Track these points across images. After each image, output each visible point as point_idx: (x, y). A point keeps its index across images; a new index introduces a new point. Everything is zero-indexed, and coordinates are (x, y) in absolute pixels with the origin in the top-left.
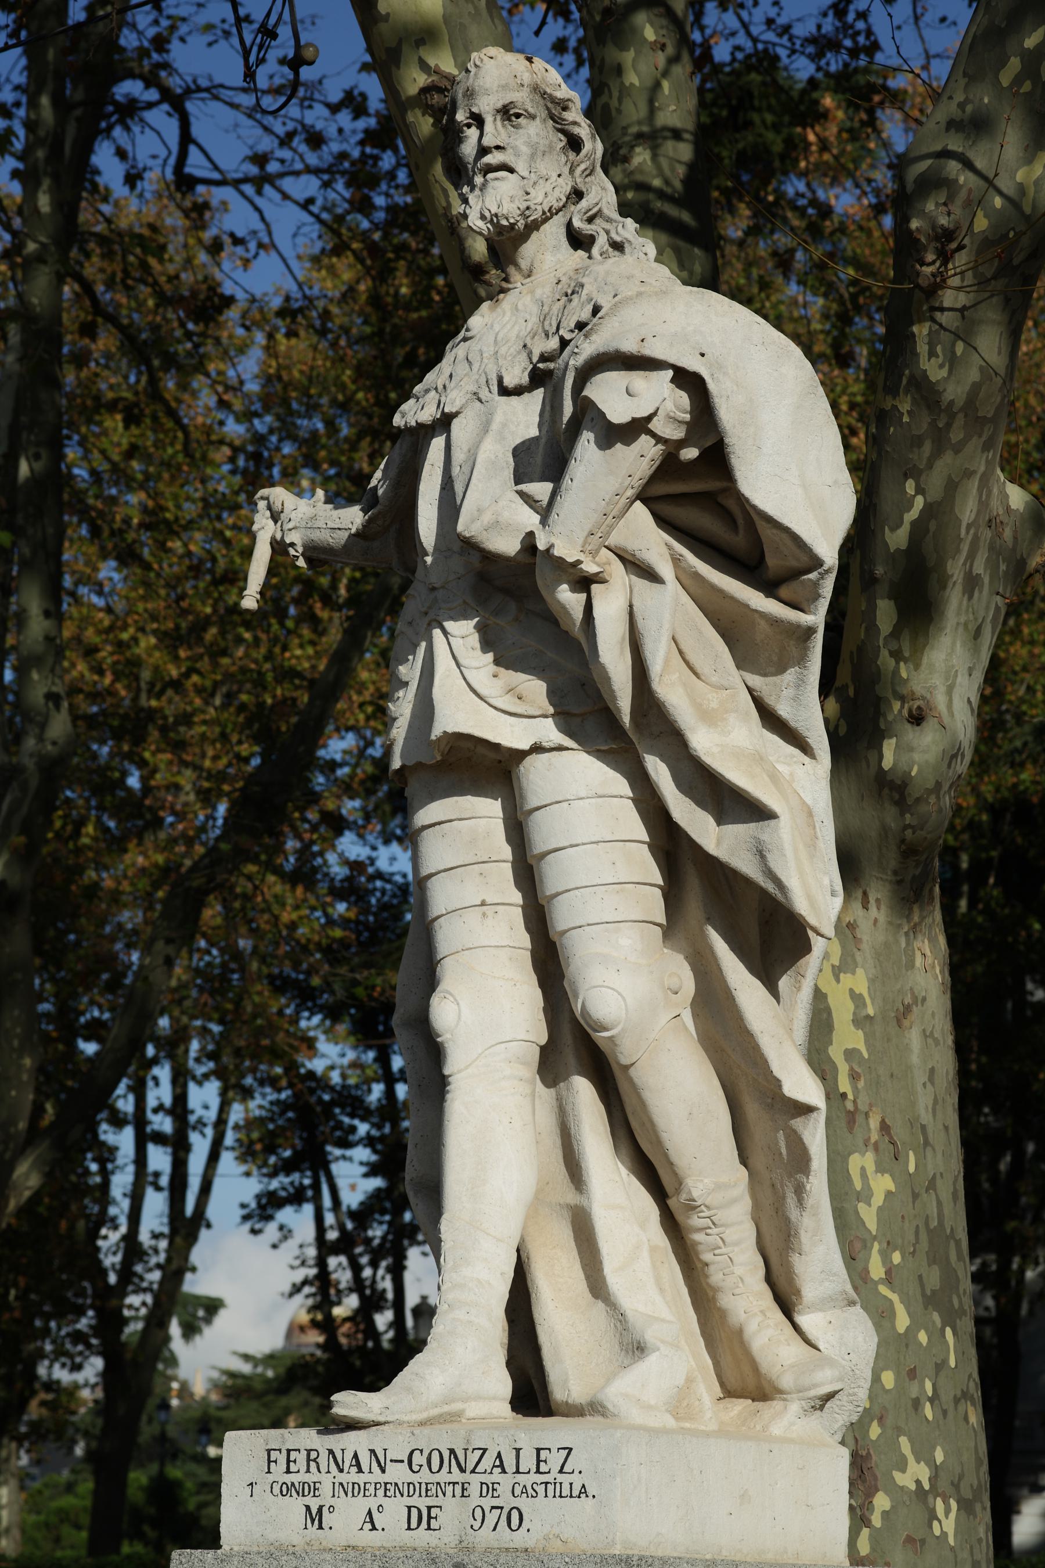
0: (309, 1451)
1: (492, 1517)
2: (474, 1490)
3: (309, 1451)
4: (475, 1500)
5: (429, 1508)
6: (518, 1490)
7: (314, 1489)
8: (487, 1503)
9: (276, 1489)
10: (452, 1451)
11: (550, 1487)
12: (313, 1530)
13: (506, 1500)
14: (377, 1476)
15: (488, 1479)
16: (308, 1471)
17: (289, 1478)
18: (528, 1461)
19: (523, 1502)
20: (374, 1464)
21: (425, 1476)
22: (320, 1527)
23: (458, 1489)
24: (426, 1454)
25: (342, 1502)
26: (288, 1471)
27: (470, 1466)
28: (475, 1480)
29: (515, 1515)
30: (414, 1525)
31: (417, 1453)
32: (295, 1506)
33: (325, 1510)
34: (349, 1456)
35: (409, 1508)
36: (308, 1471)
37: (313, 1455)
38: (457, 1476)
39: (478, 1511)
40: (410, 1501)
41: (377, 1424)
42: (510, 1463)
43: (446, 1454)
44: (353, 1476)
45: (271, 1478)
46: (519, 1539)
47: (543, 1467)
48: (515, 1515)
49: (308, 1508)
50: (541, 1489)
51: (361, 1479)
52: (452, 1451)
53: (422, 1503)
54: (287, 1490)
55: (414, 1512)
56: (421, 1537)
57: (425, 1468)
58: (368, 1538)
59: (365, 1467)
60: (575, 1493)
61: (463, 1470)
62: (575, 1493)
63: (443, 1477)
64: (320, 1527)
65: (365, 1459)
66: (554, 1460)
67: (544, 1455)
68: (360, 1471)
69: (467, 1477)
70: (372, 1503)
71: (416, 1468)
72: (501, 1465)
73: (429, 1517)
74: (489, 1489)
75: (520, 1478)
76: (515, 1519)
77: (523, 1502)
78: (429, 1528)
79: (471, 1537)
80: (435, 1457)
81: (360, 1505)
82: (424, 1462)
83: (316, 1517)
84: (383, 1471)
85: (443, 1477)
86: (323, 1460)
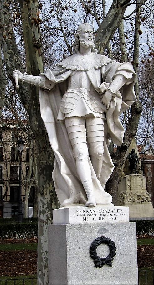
1: (112, 218)
2: (109, 215)
7: (84, 215)
8: (111, 216)
9: (78, 215)
13: (113, 216)
14: (94, 213)
17: (80, 214)
18: (116, 211)
19: (116, 216)
23: (107, 215)
25: (88, 217)
27: (108, 212)
28: (109, 213)
29: (115, 218)
32: (81, 218)
33: (86, 218)
34: (90, 211)
37: (84, 211)
38: (106, 213)
40: (99, 217)
41: (94, 206)
42: (114, 211)
43: (104, 211)
45: (77, 214)
46: (115, 221)
48: (115, 218)
51: (92, 214)
54: (80, 215)
60: (123, 215)
63: (104, 213)
66: (120, 211)
67: (118, 210)
69: (108, 213)
70: (93, 217)
77: (116, 216)
80: (103, 211)
81: (92, 217)
83: (85, 219)
85: (104, 213)
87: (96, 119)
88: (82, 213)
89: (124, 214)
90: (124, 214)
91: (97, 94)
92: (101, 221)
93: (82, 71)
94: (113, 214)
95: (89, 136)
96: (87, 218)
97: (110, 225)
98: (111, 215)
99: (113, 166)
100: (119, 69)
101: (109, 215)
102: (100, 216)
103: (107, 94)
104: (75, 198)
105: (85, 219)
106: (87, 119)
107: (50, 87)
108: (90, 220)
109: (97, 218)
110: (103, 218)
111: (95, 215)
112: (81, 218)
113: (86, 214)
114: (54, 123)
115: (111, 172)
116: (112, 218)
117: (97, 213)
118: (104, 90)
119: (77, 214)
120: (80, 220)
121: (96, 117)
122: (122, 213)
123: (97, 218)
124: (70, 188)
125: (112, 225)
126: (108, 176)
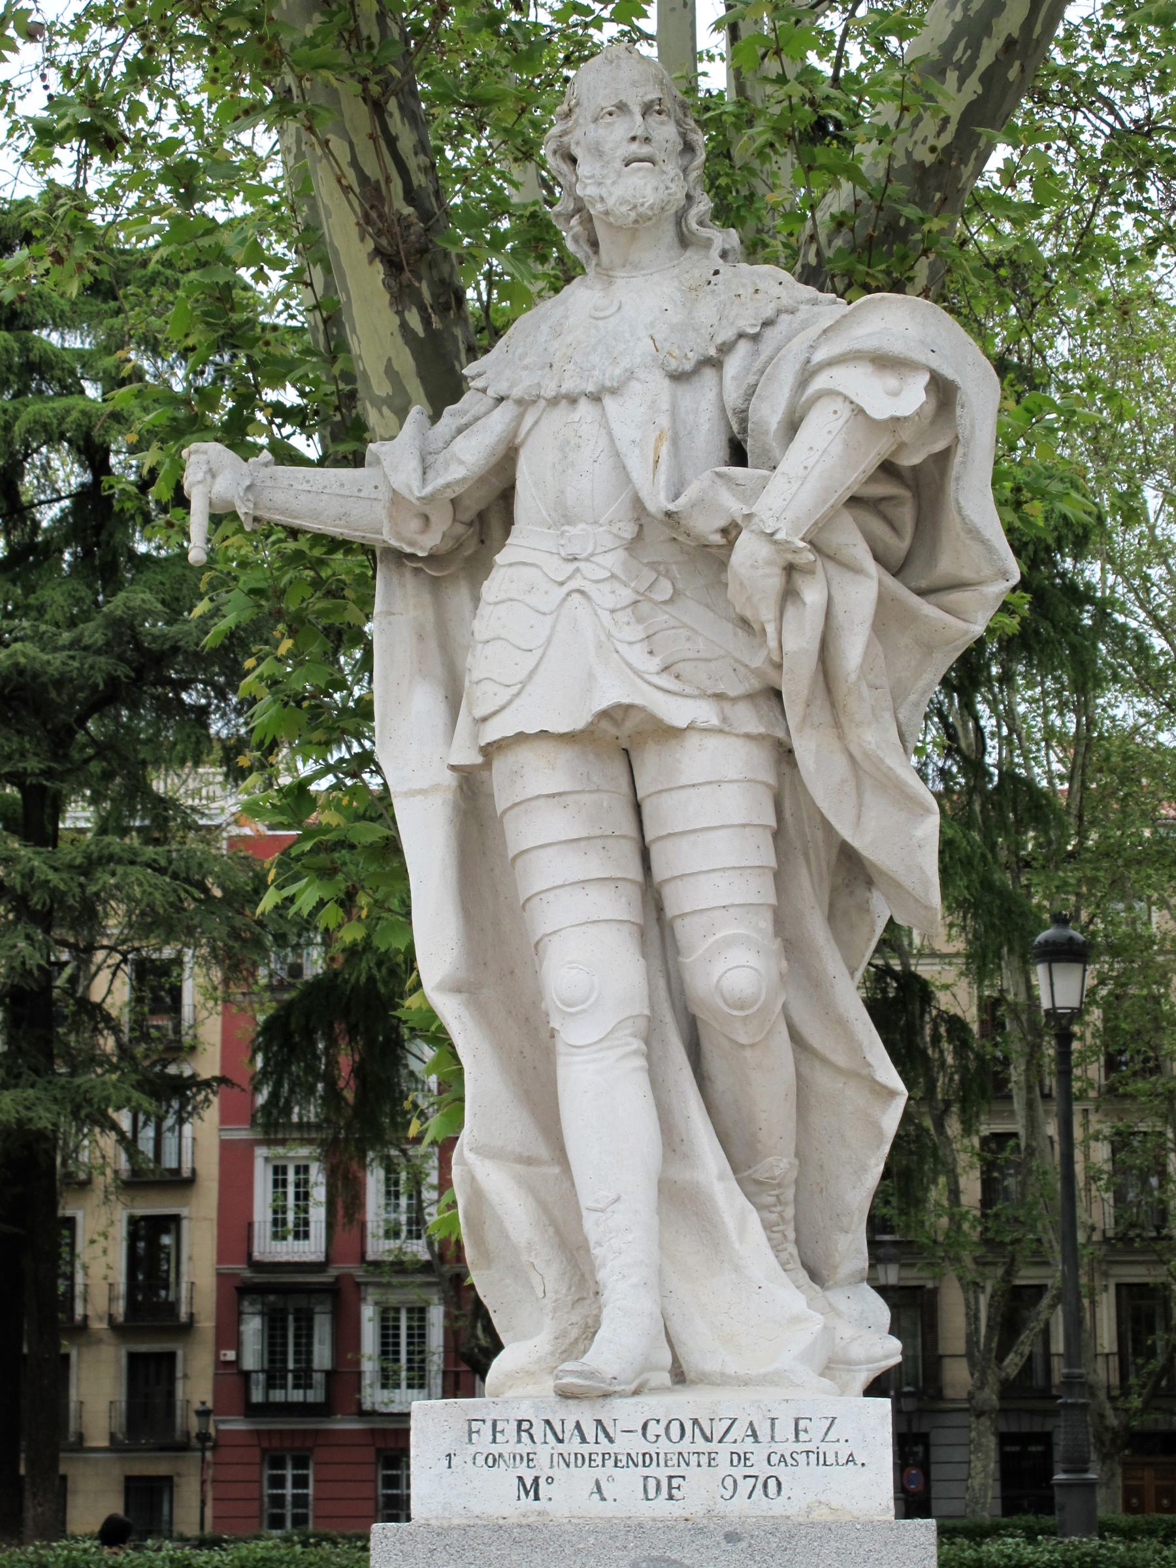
0: (520, 1422)
1: (745, 1486)
2: (723, 1459)
3: (520, 1422)
4: (724, 1467)
5: (670, 1478)
6: (775, 1459)
8: (739, 1472)
9: (480, 1460)
10: (695, 1422)
11: (813, 1457)
12: (528, 1502)
13: (761, 1469)
15: (739, 1448)
16: (519, 1441)
17: (495, 1449)
18: (785, 1430)
19: (781, 1471)
20: (601, 1435)
21: (664, 1446)
22: (537, 1498)
23: (704, 1460)
24: (663, 1423)
25: (560, 1472)
26: (494, 1441)
27: (716, 1437)
28: (723, 1452)
29: (772, 1483)
30: (652, 1493)
31: (652, 1424)
33: (542, 1481)
34: (570, 1425)
35: (646, 1478)
36: (519, 1441)
37: (525, 1426)
38: (701, 1445)
39: (729, 1482)
42: (763, 1431)
44: (573, 1445)
45: (472, 1449)
46: (777, 1506)
47: (803, 1436)
48: (772, 1483)
49: (520, 1478)
50: (802, 1458)
51: (585, 1449)
52: (695, 1422)
53: (662, 1473)
54: (494, 1460)
55: (652, 1484)
56: (661, 1507)
57: (663, 1437)
58: (594, 1508)
59: (590, 1437)
60: (842, 1460)
61: (708, 1439)
62: (841, 1462)
63: (685, 1446)
64: (537, 1498)
65: (589, 1430)
66: (816, 1429)
68: (584, 1440)
69: (714, 1446)
70: (599, 1473)
71: (652, 1438)
72: (754, 1435)
73: (670, 1487)
74: (743, 1458)
75: (775, 1447)
76: (770, 1486)
77: (781, 1471)
78: (671, 1497)
79: (721, 1507)
80: (675, 1427)
81: (585, 1476)
82: (662, 1432)
83: (533, 1489)
84: (611, 1440)
85: (685, 1446)
86: (538, 1430)
87: (693, 740)
88: (508, 1445)
89: (851, 1459)
90: (851, 1459)
91: (685, 552)
92: (661, 1507)
93: (573, 400)
94: (758, 1454)
95: (660, 872)
96: (550, 1480)
97: (720, 1538)
98: (743, 1458)
99: (892, 1094)
100: (819, 356)
101: (723, 1459)
102: (652, 1471)
103: (748, 552)
104: (563, 1334)
105: (533, 1489)
106: (621, 742)
107: (419, 538)
108: (569, 1496)
109: (625, 1486)
110: (675, 1482)
111: (610, 1463)
112: (505, 1479)
113: (544, 1451)
114: (450, 796)
115: (880, 1133)
116: (745, 1486)
117: (636, 1445)
118: (722, 523)
119: (472, 1449)
120: (495, 1496)
121: (682, 724)
122: (829, 1449)
123: (625, 1486)
124: (524, 1257)
125: (732, 1537)
126: (864, 1169)
